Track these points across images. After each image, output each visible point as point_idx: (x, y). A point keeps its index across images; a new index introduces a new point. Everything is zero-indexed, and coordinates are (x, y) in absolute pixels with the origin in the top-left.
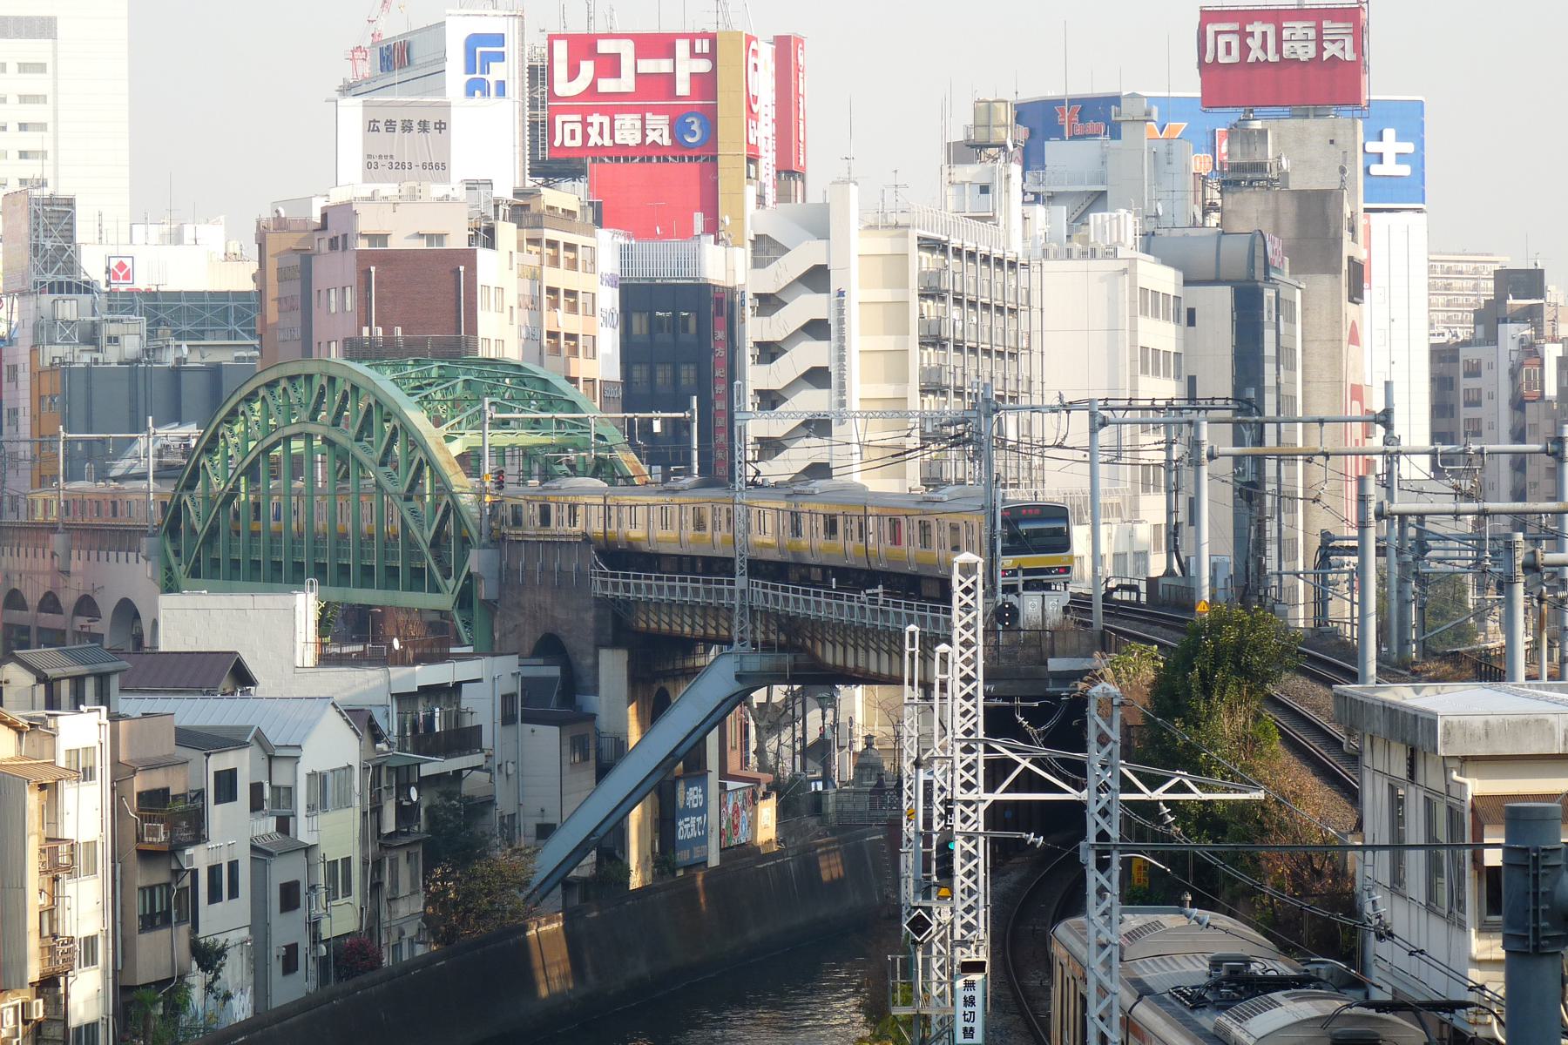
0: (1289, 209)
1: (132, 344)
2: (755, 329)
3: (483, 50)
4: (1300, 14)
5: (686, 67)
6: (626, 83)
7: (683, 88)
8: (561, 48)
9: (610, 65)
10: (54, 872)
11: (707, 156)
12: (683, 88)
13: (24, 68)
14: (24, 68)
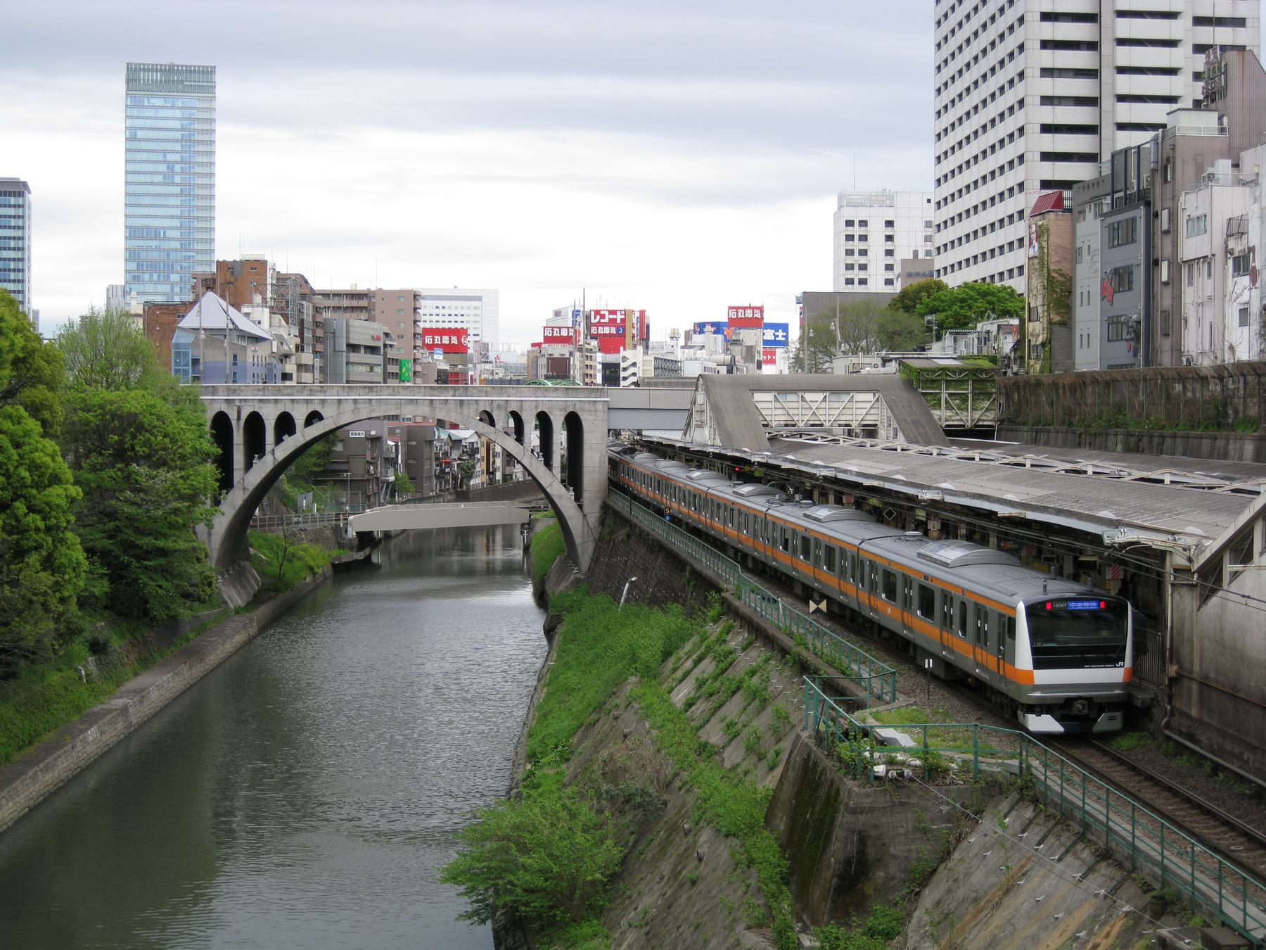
0: (744, 349)
1: (501, 375)
2: (623, 374)
4: (750, 307)
5: (619, 317)
6: (607, 320)
7: (619, 321)
8: (593, 313)
9: (603, 316)
10: (494, 457)
11: (624, 335)
12: (619, 321)
13: (475, 308)
14: (475, 308)
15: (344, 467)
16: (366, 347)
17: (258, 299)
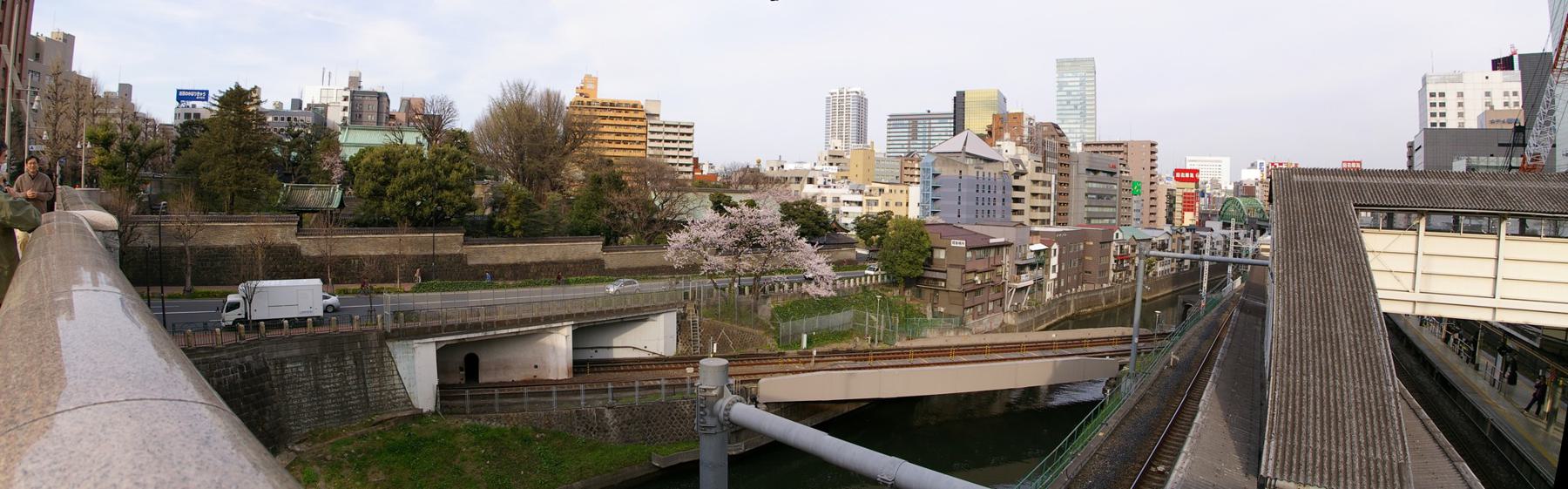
1: (1223, 195)
3: (1261, 164)
15: (942, 276)
16: (1104, 172)
17: (1007, 135)
